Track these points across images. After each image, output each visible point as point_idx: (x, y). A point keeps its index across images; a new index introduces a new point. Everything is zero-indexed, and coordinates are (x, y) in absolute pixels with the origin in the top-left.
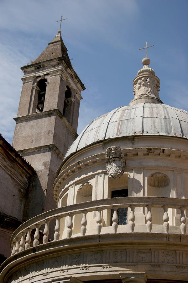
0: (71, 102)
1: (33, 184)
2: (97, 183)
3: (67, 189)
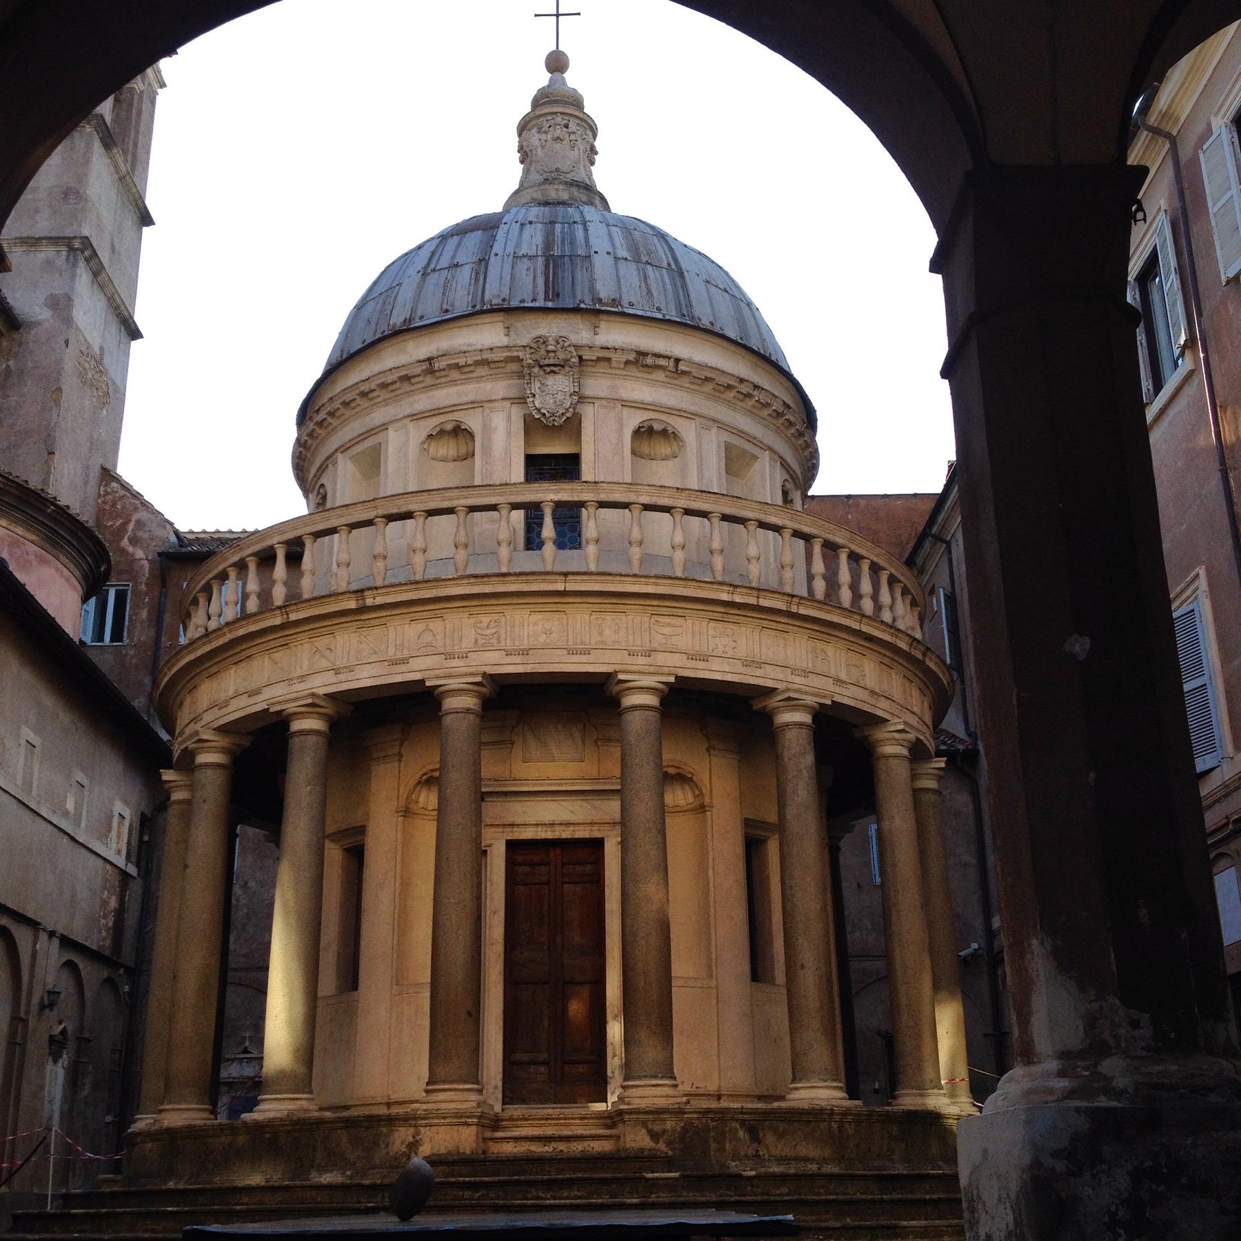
0: (132, 96)
1: (11, 363)
2: (487, 429)
3: (384, 427)
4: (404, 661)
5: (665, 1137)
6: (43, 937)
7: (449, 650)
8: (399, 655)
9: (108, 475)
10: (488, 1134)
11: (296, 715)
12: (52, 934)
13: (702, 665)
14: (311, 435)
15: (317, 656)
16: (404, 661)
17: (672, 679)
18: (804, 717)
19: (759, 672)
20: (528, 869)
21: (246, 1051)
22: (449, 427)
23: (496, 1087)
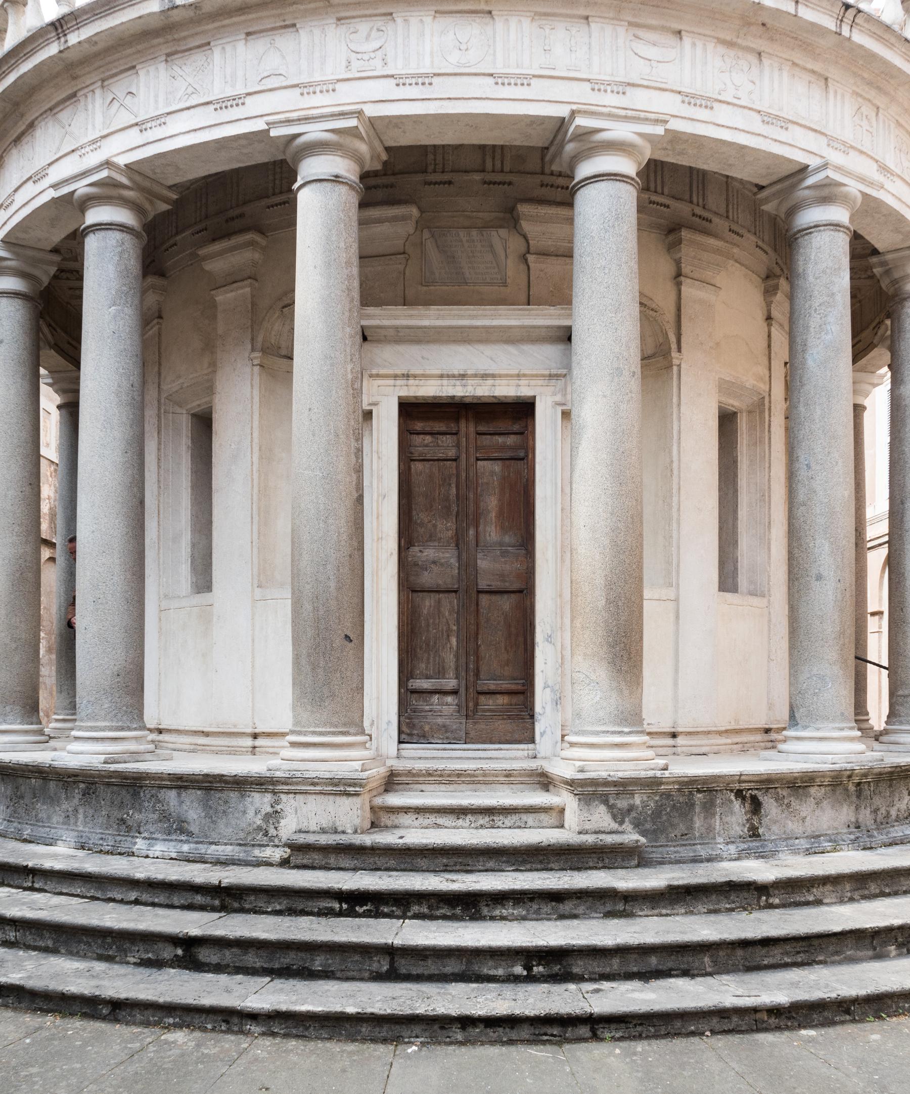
4: (236, 101)
5: (633, 814)
7: (304, 79)
8: (229, 92)
10: (379, 801)
13: (703, 114)
15: (116, 104)
16: (236, 101)
20: (428, 439)
23: (389, 722)
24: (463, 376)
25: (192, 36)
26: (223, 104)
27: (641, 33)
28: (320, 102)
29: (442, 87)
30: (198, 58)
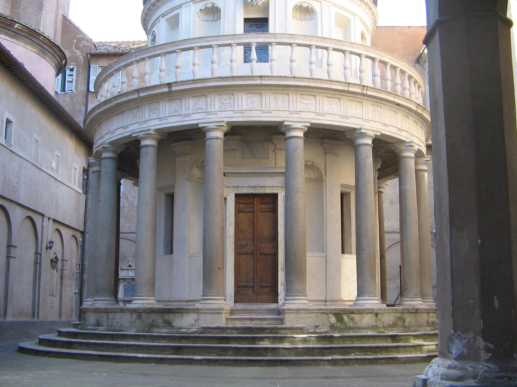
6: (46, 219)
7: (209, 110)
8: (187, 112)
9: (65, 19)
10: (228, 317)
11: (144, 138)
12: (49, 219)
13: (323, 118)
14: (149, 10)
15: (152, 112)
17: (309, 125)
18: (370, 142)
19: (348, 121)
21: (130, 266)
22: (210, 5)
24: (255, 187)
25: (177, 96)
26: (186, 115)
27: (303, 96)
28: (214, 118)
29: (246, 114)
30: (178, 102)
